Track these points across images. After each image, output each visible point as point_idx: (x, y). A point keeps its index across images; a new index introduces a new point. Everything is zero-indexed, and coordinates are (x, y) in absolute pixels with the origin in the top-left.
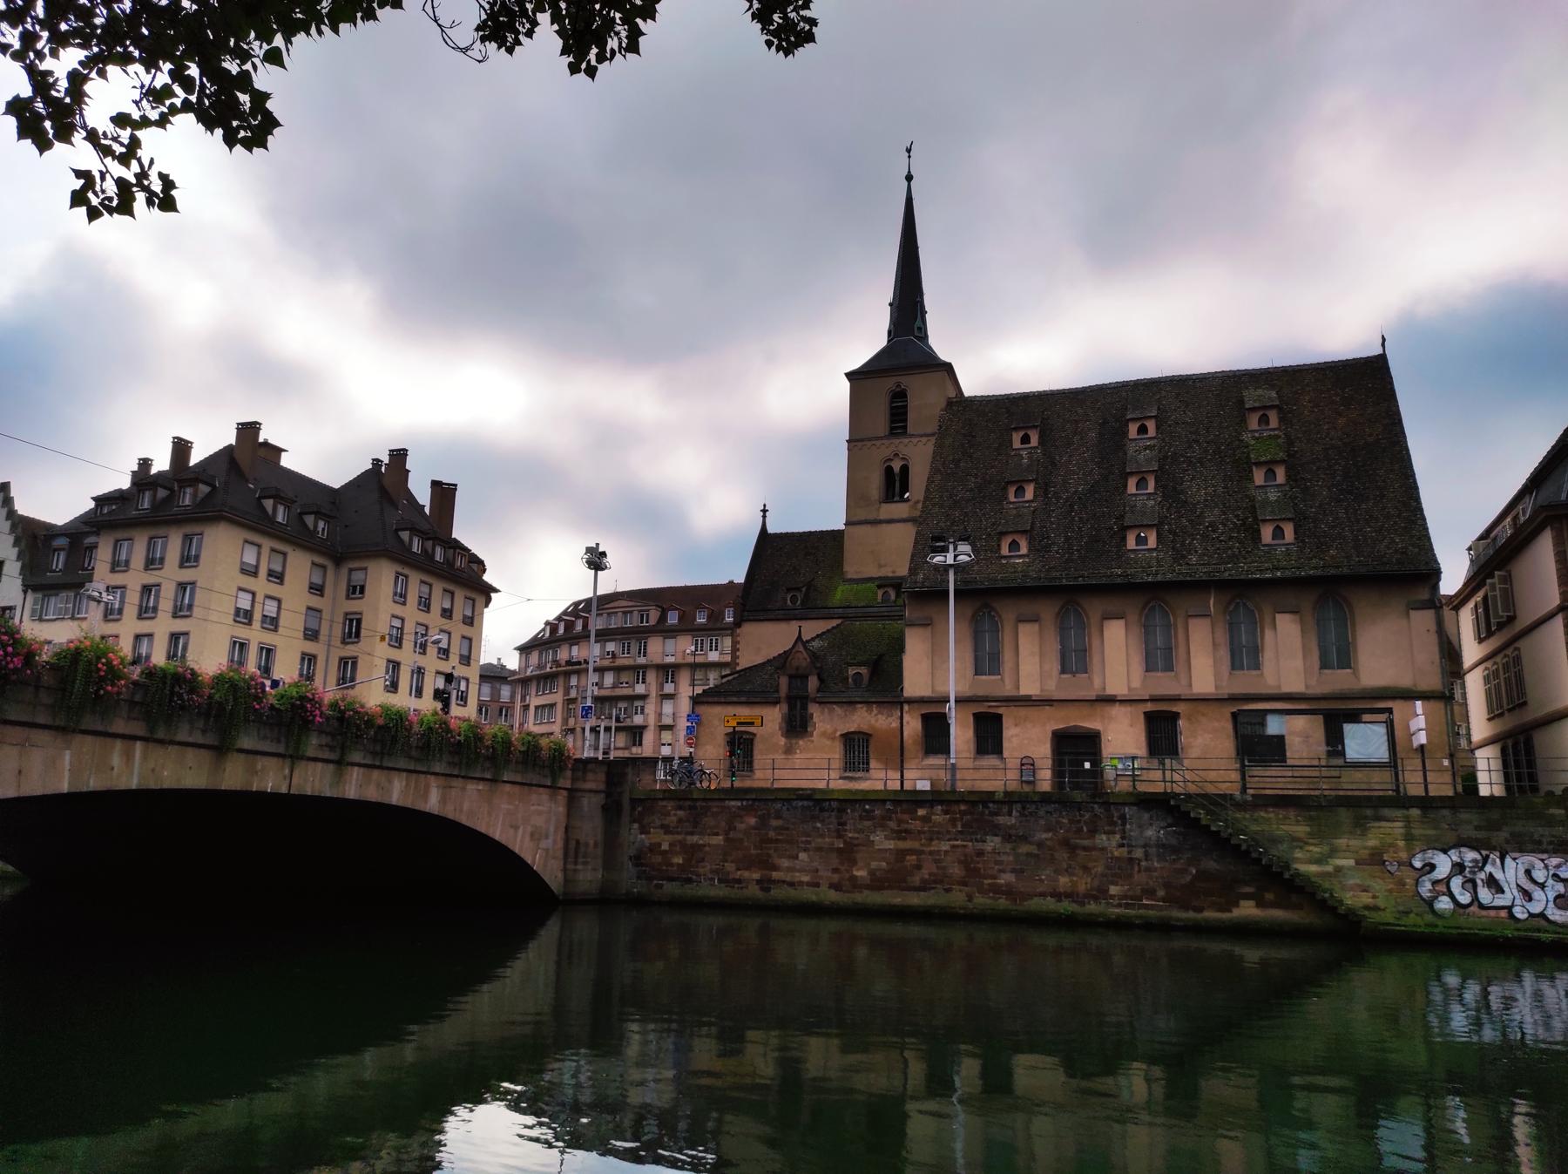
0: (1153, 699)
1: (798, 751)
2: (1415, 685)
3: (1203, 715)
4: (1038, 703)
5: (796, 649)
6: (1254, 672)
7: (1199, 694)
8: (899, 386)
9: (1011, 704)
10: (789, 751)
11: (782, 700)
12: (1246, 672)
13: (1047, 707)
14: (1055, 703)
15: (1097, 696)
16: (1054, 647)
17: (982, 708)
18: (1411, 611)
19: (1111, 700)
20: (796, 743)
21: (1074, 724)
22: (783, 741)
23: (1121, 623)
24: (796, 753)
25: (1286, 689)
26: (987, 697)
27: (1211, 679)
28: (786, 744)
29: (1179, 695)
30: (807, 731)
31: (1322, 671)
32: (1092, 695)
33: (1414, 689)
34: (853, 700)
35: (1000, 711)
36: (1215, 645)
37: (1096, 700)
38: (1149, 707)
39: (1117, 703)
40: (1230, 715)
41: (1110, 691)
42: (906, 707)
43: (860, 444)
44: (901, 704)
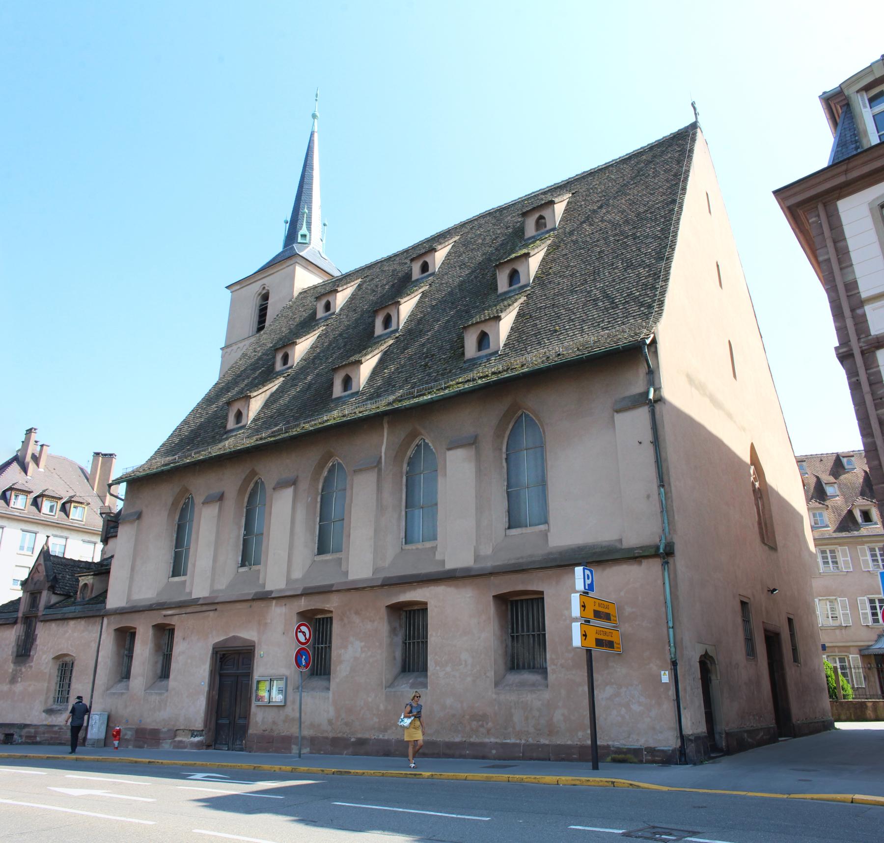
0: (308, 593)
1: (19, 679)
2: (620, 541)
3: (357, 613)
4: (205, 608)
5: (38, 562)
6: (428, 545)
7: (354, 582)
8: (264, 288)
9: (183, 611)
10: (13, 680)
11: (19, 620)
12: (420, 546)
13: (211, 613)
14: (218, 607)
15: (256, 594)
16: (234, 534)
17: (158, 618)
18: (617, 416)
19: (264, 597)
20: (20, 670)
21: (231, 635)
22: (10, 667)
23: (289, 492)
24: (17, 682)
25: (449, 566)
26: (164, 603)
27: (369, 557)
28: (13, 671)
29: (332, 585)
30: (29, 656)
31: (508, 531)
32: (250, 591)
33: (619, 546)
34: (66, 616)
35: (174, 621)
36: (380, 508)
37: (253, 600)
38: (304, 604)
39: (274, 602)
40: (385, 608)
41: (268, 588)
42: (105, 620)
43: (229, 350)
44: (103, 617)
